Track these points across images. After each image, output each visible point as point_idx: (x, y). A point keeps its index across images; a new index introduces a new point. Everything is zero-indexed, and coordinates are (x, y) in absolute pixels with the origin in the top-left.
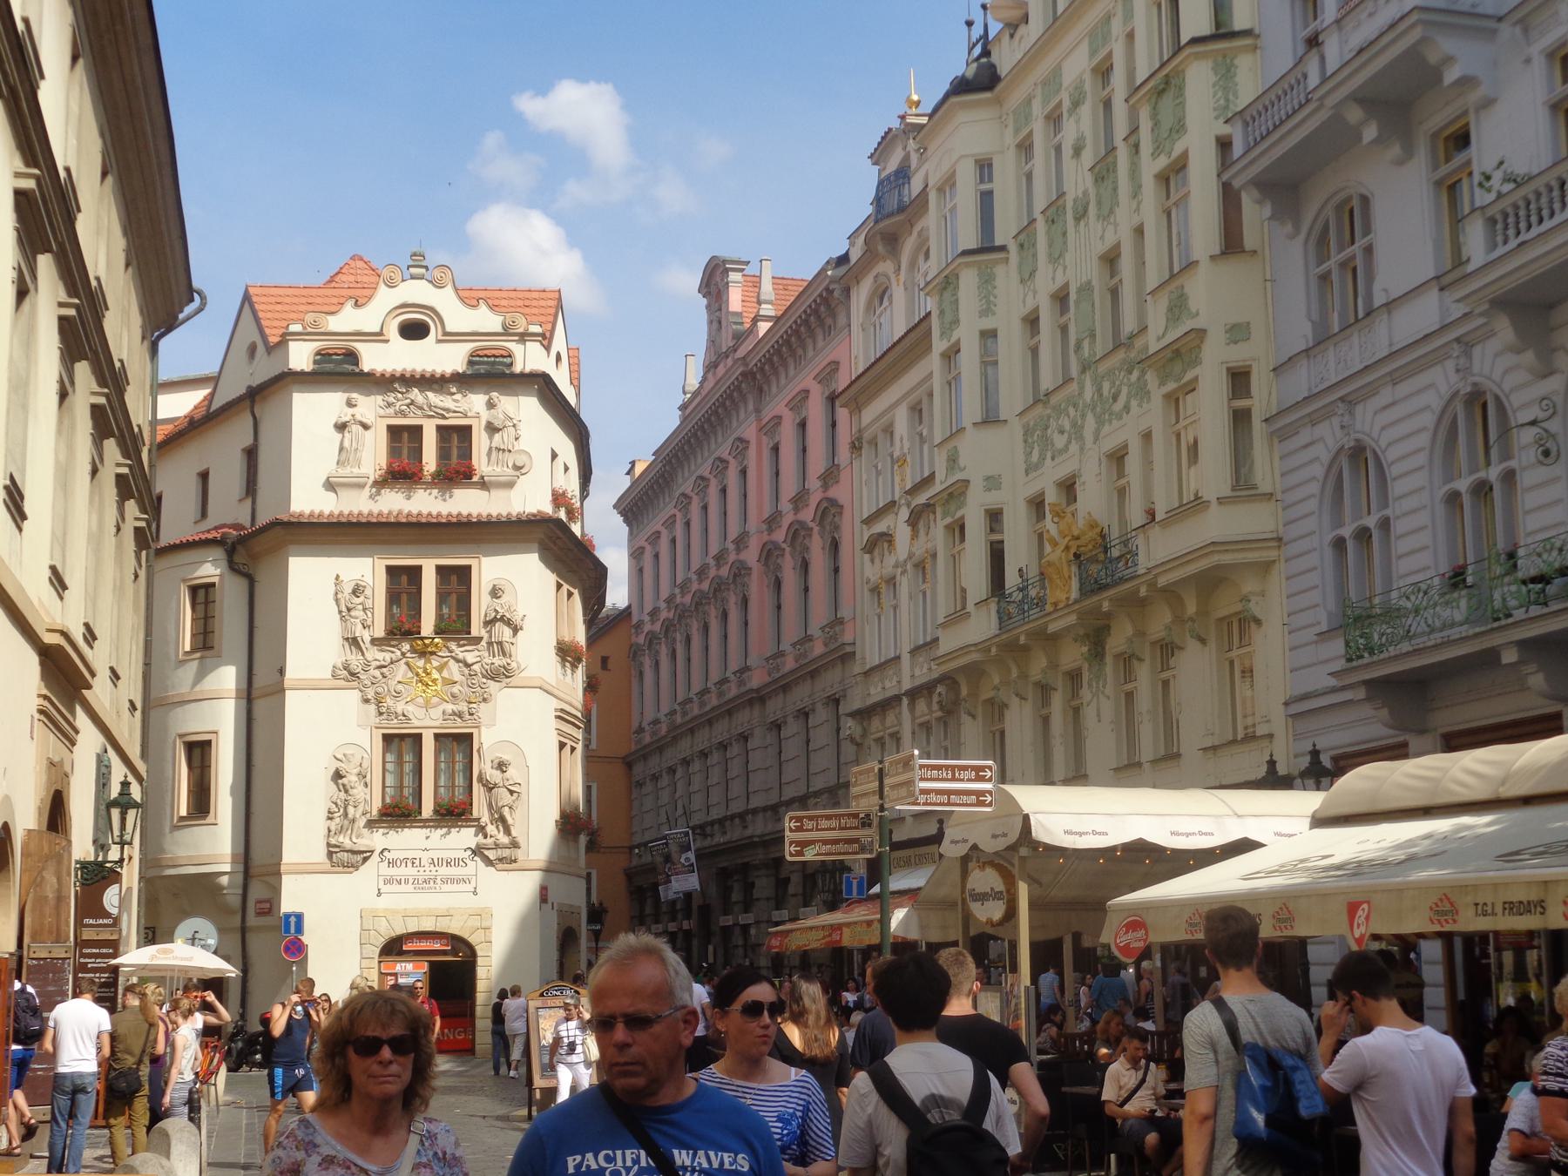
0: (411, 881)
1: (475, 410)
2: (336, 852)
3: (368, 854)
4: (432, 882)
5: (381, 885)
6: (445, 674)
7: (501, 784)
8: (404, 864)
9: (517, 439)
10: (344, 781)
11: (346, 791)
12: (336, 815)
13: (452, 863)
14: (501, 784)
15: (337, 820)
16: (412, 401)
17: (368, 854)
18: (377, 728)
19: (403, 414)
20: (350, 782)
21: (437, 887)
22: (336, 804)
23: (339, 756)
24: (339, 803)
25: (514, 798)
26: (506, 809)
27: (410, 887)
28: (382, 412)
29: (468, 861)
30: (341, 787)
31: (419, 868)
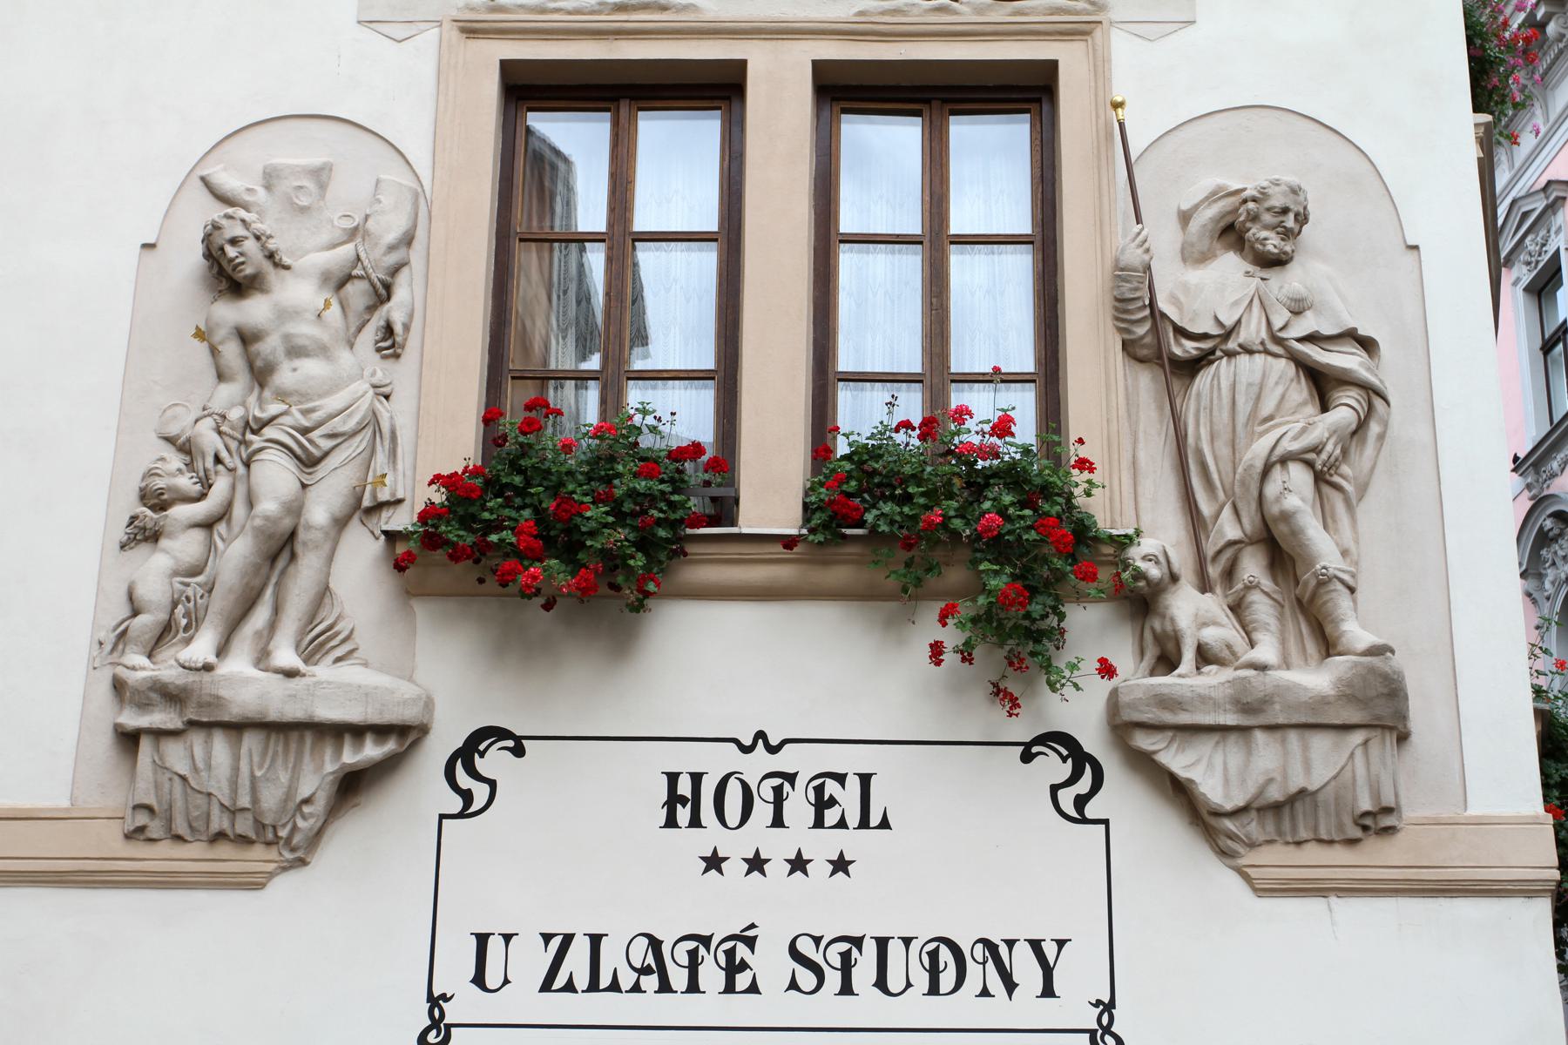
2: (159, 734)
3: (372, 751)
7: (1254, 331)
10: (254, 310)
11: (260, 375)
12: (182, 512)
14: (1254, 331)
15: (184, 546)
17: (372, 751)
18: (471, 31)
20: (285, 314)
22: (186, 448)
23: (230, 182)
24: (209, 440)
25: (1343, 414)
26: (1299, 476)
30: (231, 352)
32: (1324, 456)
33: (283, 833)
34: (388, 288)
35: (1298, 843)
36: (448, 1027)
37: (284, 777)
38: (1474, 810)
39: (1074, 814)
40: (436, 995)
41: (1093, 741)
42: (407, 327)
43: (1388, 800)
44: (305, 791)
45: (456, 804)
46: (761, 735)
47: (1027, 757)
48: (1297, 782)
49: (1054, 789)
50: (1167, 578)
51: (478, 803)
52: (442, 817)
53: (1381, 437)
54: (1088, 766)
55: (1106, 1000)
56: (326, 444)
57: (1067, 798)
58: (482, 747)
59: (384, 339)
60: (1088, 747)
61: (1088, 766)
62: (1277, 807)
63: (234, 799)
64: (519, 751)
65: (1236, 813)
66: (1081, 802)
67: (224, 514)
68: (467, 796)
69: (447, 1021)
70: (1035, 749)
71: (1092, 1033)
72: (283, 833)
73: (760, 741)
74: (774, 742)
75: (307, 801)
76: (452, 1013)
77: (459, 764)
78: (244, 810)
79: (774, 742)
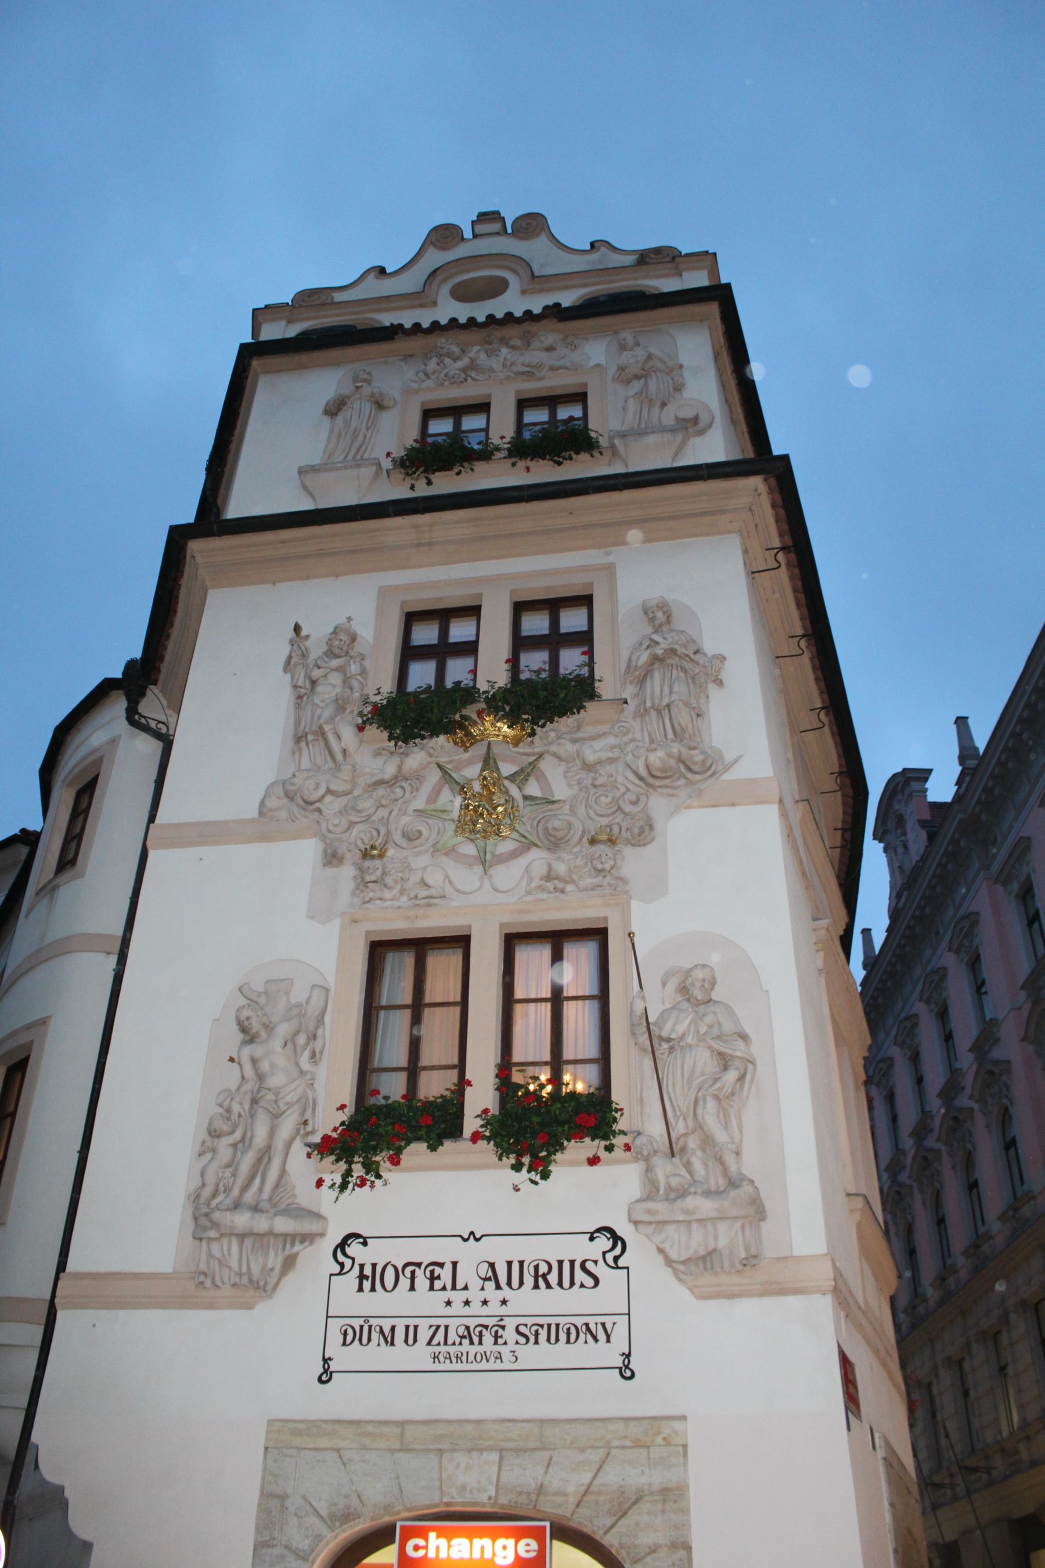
0: (424, 1335)
1: (592, 363)
2: (210, 1240)
4: (488, 1338)
5: (334, 1348)
6: (533, 788)
8: (404, 1282)
9: (679, 388)
13: (553, 1278)
16: (472, 360)
19: (455, 381)
21: (503, 1349)
27: (420, 1355)
28: (415, 386)
29: (600, 1270)
31: (449, 1294)
32: (723, 1092)
33: (262, 1284)
34: (315, 1037)
35: (716, 1274)
36: (331, 1373)
37: (261, 1260)
38: (796, 1252)
39: (612, 1264)
40: (326, 1357)
41: (623, 1229)
42: (322, 1052)
43: (753, 1252)
44: (270, 1265)
45: (337, 1269)
46: (472, 1233)
47: (592, 1239)
48: (711, 1246)
49: (604, 1253)
50: (652, 1153)
51: (346, 1269)
52: (331, 1275)
53: (752, 1080)
54: (619, 1243)
55: (627, 1352)
56: (283, 1108)
57: (610, 1257)
58: (349, 1242)
59: (312, 1058)
60: (619, 1234)
61: (619, 1243)
62: (703, 1258)
63: (240, 1269)
64: (365, 1244)
65: (683, 1262)
66: (616, 1259)
67: (243, 1140)
68: (342, 1265)
69: (331, 1369)
70: (595, 1235)
71: (620, 1368)
72: (262, 1284)
73: (472, 1236)
74: (478, 1236)
75: (272, 1270)
76: (333, 1366)
77: (339, 1250)
78: (244, 1274)
79: (478, 1236)
